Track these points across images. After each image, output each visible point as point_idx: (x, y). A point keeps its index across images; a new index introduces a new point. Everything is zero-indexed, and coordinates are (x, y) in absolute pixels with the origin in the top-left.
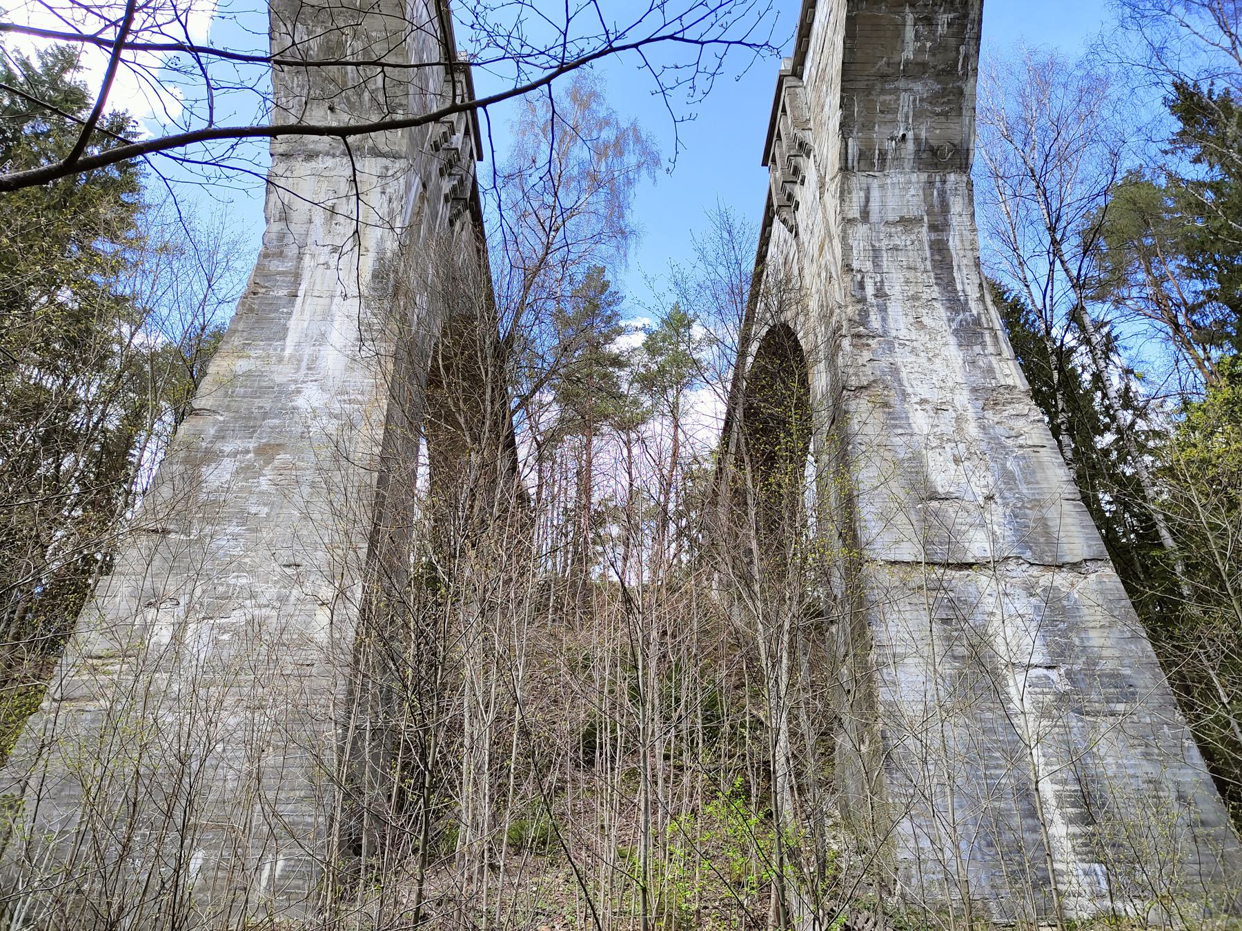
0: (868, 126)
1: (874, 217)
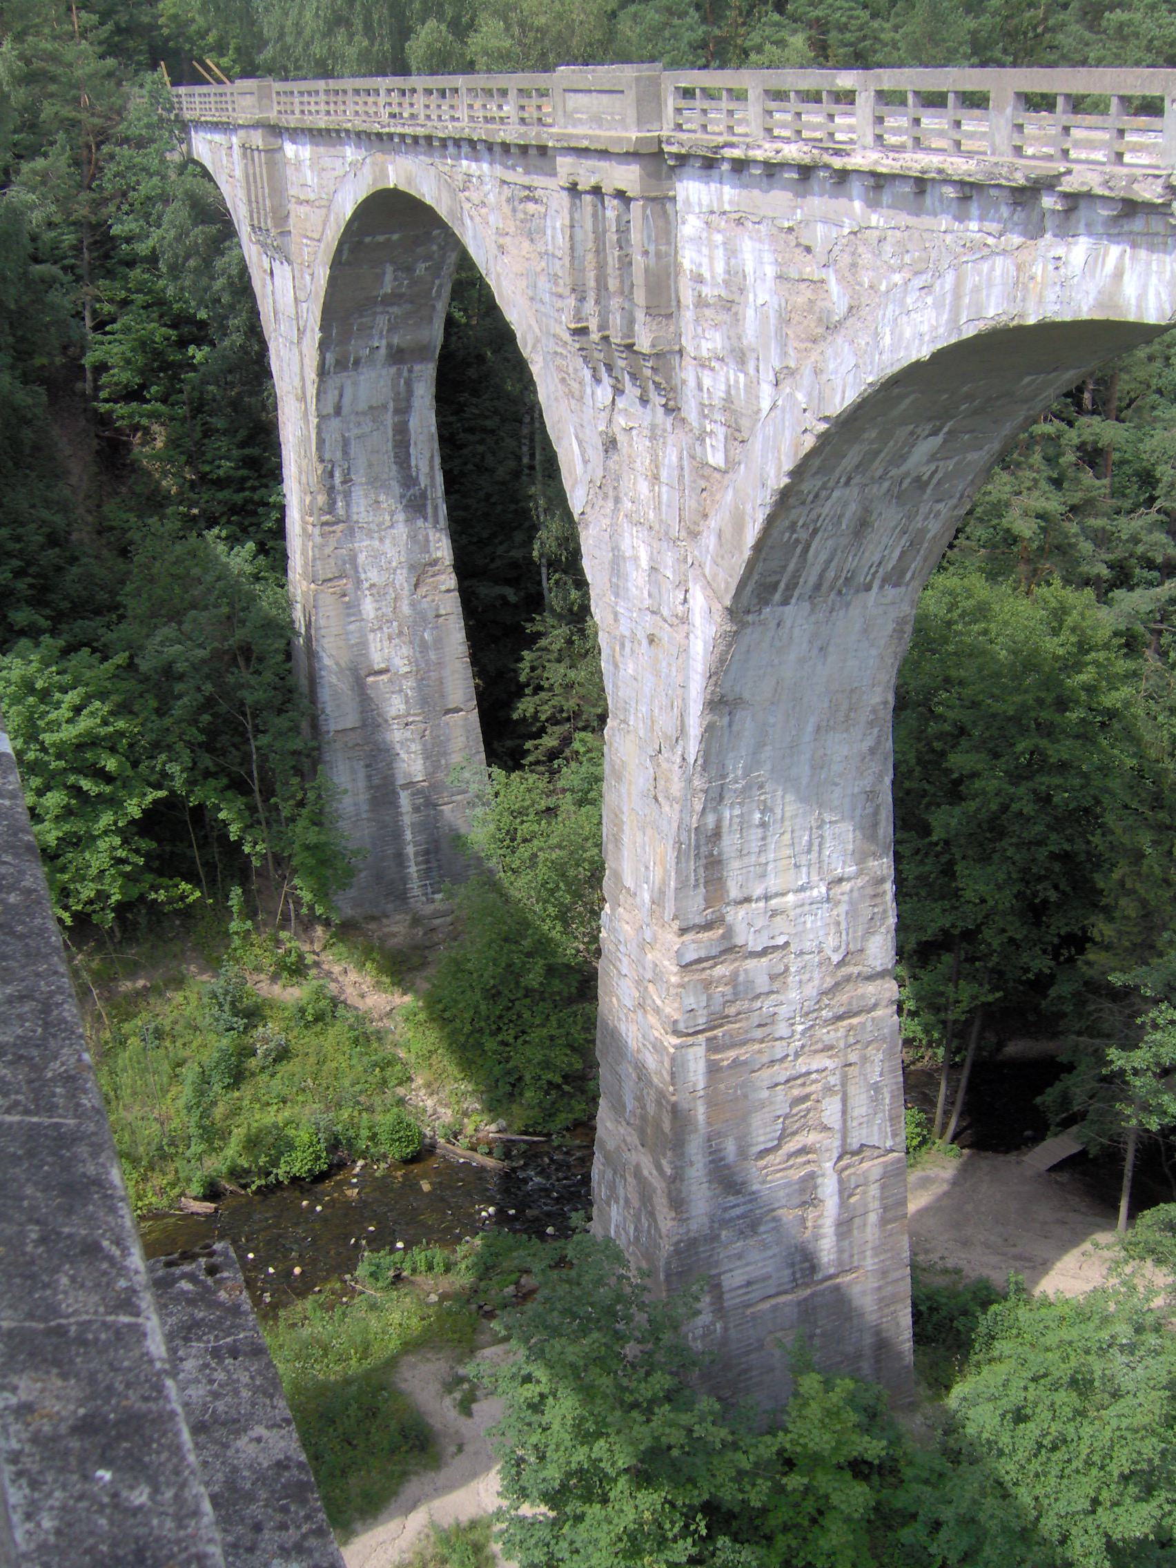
0: (345, 338)
1: (345, 411)
